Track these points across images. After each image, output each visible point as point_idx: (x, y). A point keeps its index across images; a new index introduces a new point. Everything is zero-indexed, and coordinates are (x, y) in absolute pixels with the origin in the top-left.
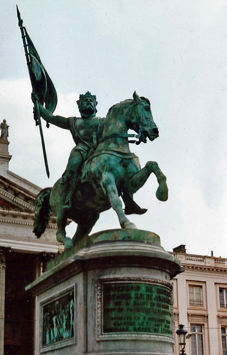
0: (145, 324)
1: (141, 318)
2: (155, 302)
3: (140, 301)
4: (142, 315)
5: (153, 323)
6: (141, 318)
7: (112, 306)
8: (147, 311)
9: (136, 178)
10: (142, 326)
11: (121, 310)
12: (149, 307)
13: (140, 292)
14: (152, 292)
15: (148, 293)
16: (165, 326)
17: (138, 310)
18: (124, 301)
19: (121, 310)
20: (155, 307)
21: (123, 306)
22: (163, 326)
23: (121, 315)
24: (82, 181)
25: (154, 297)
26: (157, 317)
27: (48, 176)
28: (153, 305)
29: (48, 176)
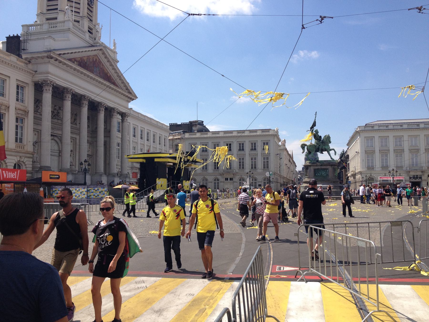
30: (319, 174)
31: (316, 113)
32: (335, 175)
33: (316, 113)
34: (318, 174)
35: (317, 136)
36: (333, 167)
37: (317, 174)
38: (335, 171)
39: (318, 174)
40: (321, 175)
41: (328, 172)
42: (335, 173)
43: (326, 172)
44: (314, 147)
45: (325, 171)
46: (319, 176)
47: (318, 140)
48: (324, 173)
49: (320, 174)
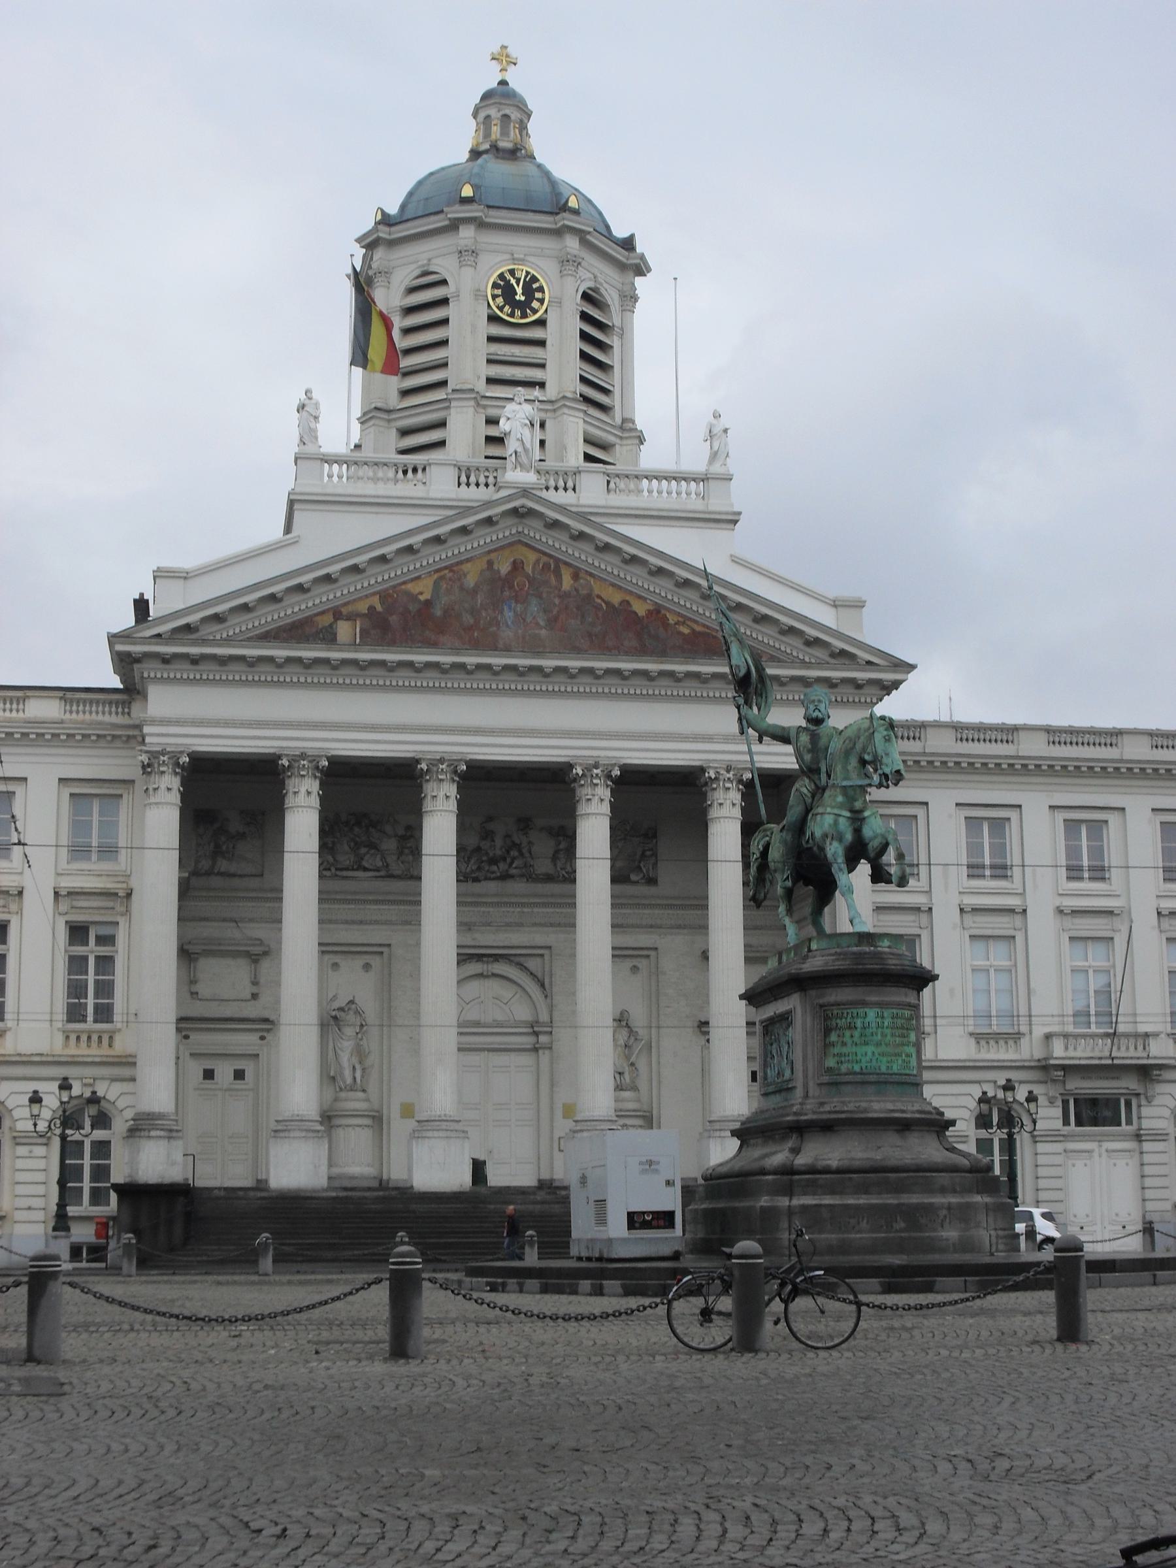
0: (874, 1061)
1: (869, 1054)
2: (888, 1031)
3: (868, 1032)
4: (870, 1049)
5: (885, 1059)
6: (869, 1054)
7: (833, 1037)
8: (878, 1044)
10: (869, 1065)
11: (844, 1044)
12: (879, 1037)
13: (867, 1020)
14: (883, 1017)
15: (878, 1020)
16: (904, 1061)
17: (866, 1044)
18: (848, 1033)
19: (844, 1044)
20: (889, 1037)
21: (847, 1039)
22: (900, 1062)
23: (845, 1050)
25: (886, 1024)
26: (889, 1050)
28: (884, 1035)
32: (831, 1062)
38: (827, 1031)
42: (827, 1046)
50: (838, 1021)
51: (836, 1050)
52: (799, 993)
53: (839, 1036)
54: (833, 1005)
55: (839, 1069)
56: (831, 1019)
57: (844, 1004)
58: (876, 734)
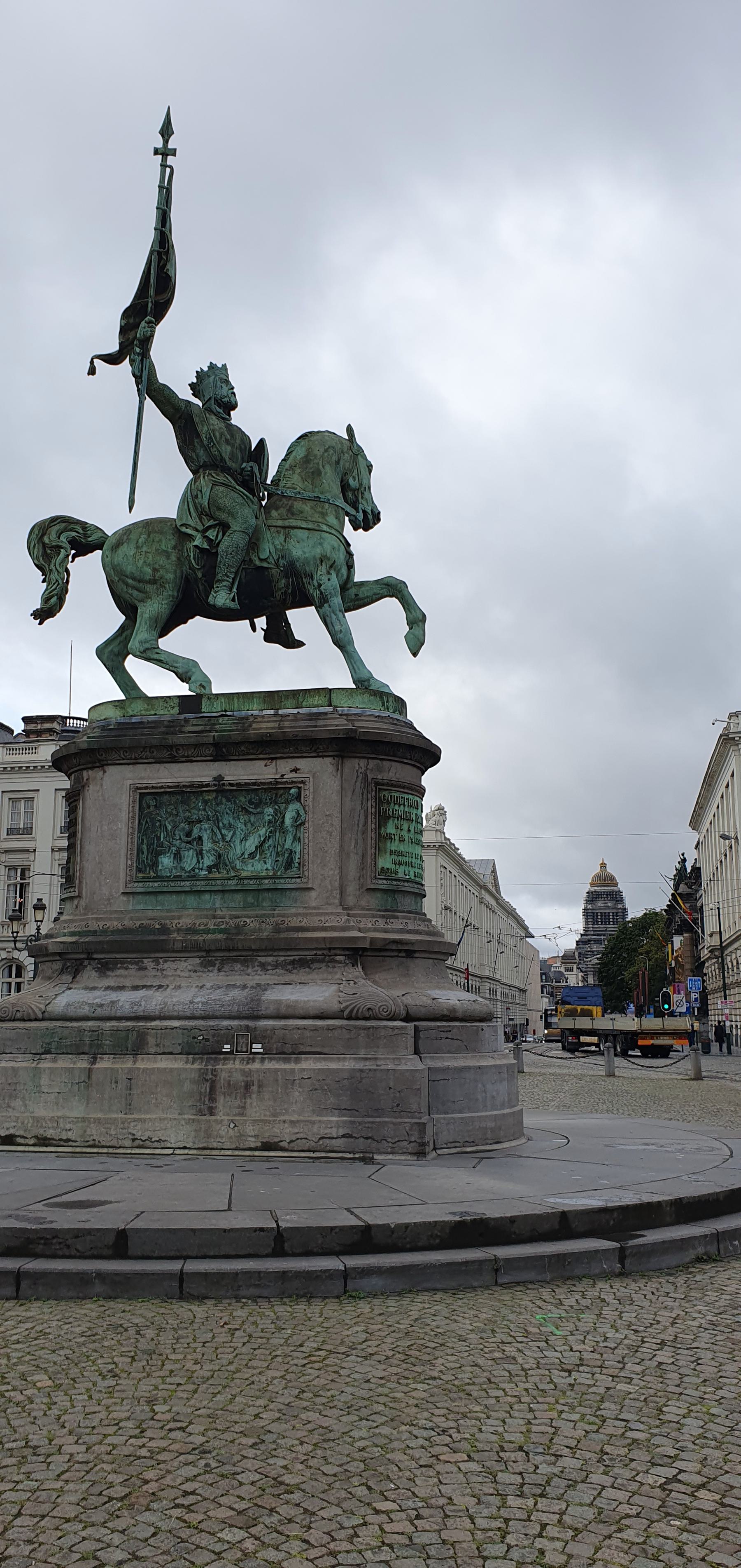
7: (391, 829)
9: (356, 595)
11: (402, 840)
19: (402, 840)
23: (402, 848)
24: (258, 563)
27: (131, 508)
29: (131, 508)
30: (189, 860)
31: (166, 131)
32: (386, 862)
33: (166, 131)
34: (178, 856)
35: (203, 430)
36: (355, 765)
37: (166, 861)
38: (383, 818)
39: (178, 856)
40: (220, 862)
41: (299, 824)
42: (383, 838)
43: (277, 825)
44: (168, 542)
45: (270, 810)
46: (192, 876)
47: (226, 470)
48: (251, 844)
49: (208, 861)
50: (397, 807)
51: (394, 846)
52: (328, 760)
53: (397, 828)
54: (392, 785)
55: (396, 873)
56: (389, 803)
57: (404, 787)
58: (359, 457)
